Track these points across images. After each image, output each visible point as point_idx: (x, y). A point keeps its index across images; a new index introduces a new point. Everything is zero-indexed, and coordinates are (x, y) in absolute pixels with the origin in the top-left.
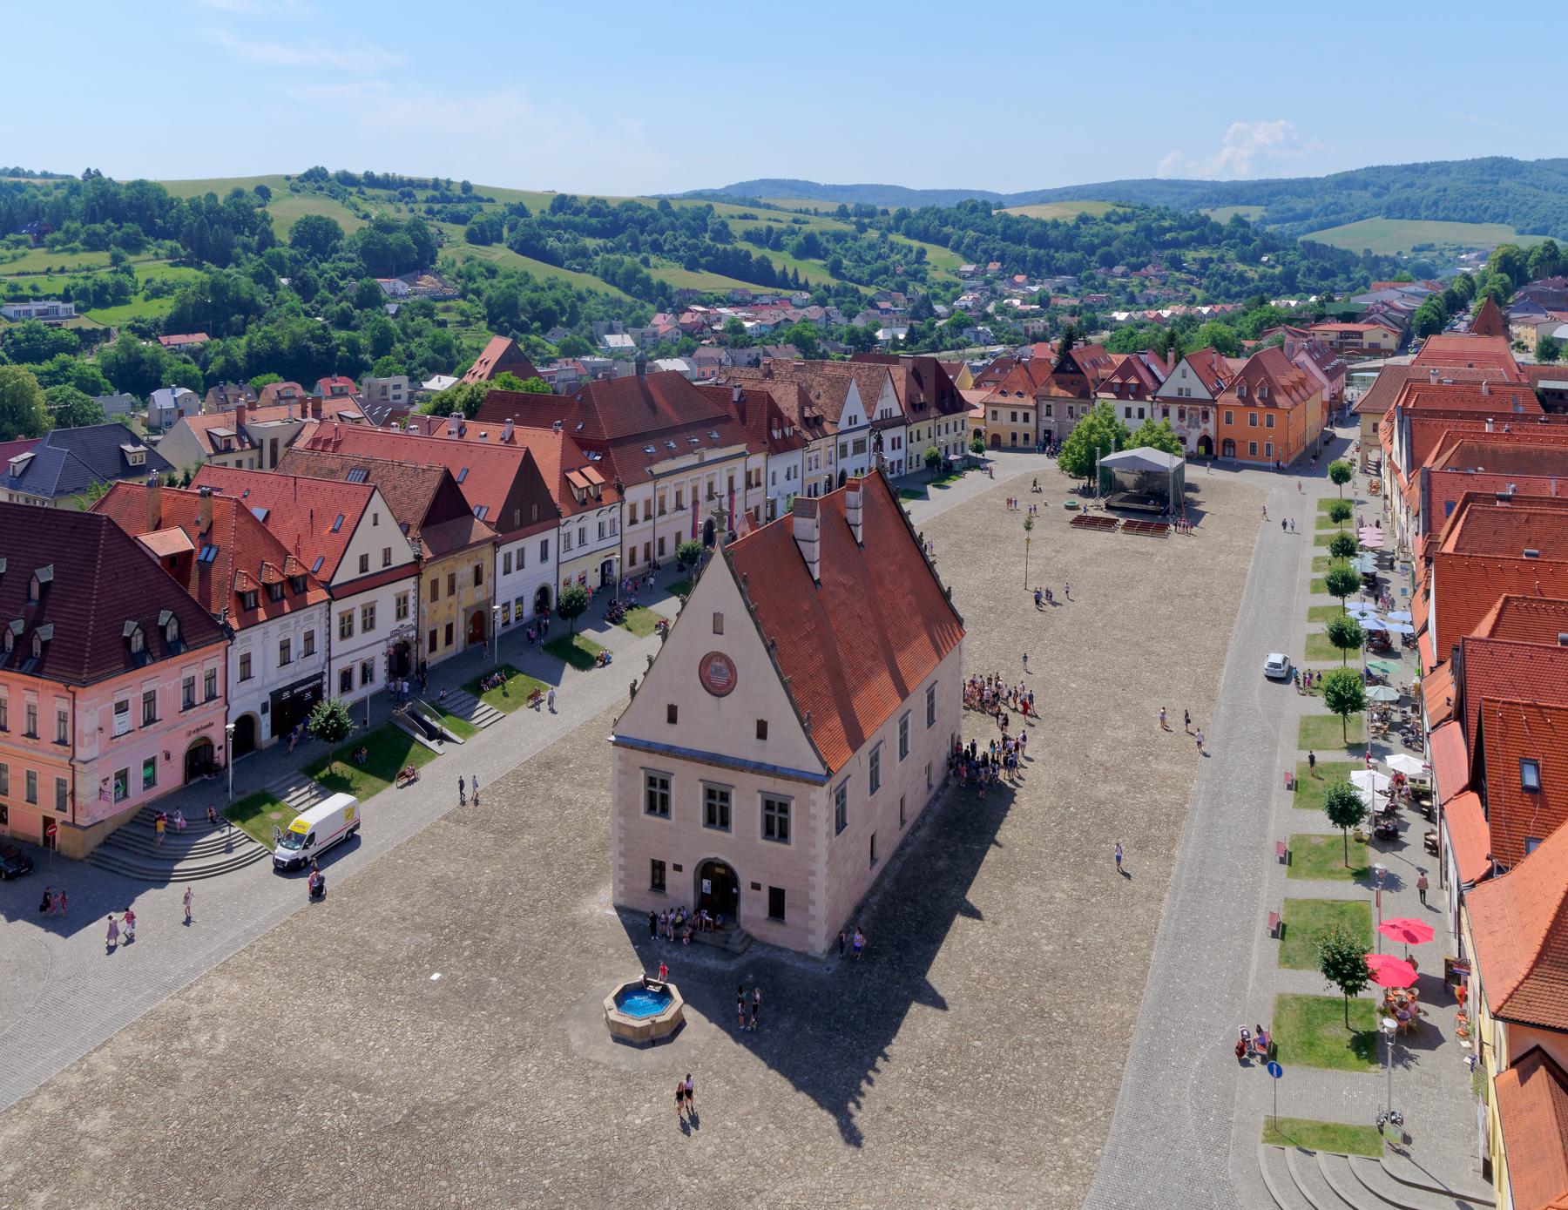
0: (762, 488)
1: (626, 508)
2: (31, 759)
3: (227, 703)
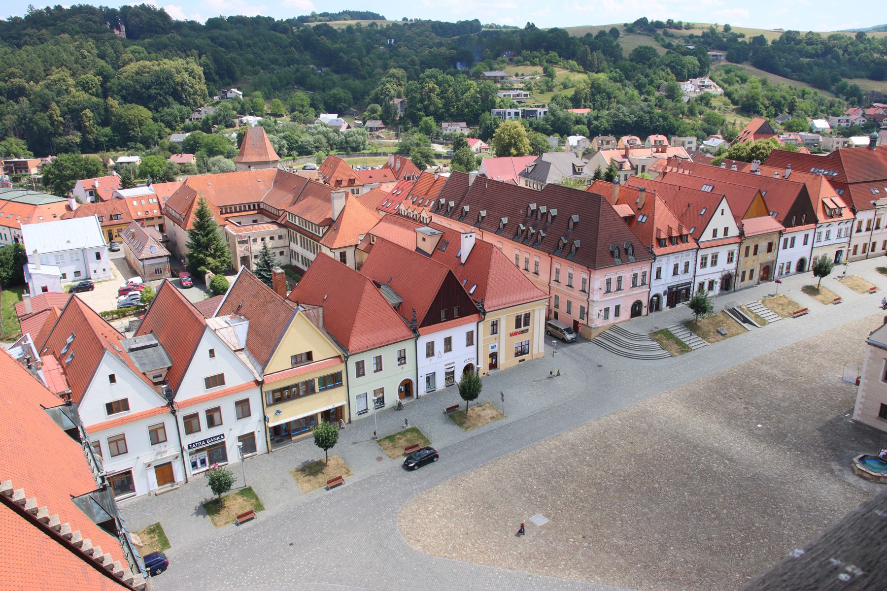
1: (856, 223)
2: (569, 295)
3: (650, 288)
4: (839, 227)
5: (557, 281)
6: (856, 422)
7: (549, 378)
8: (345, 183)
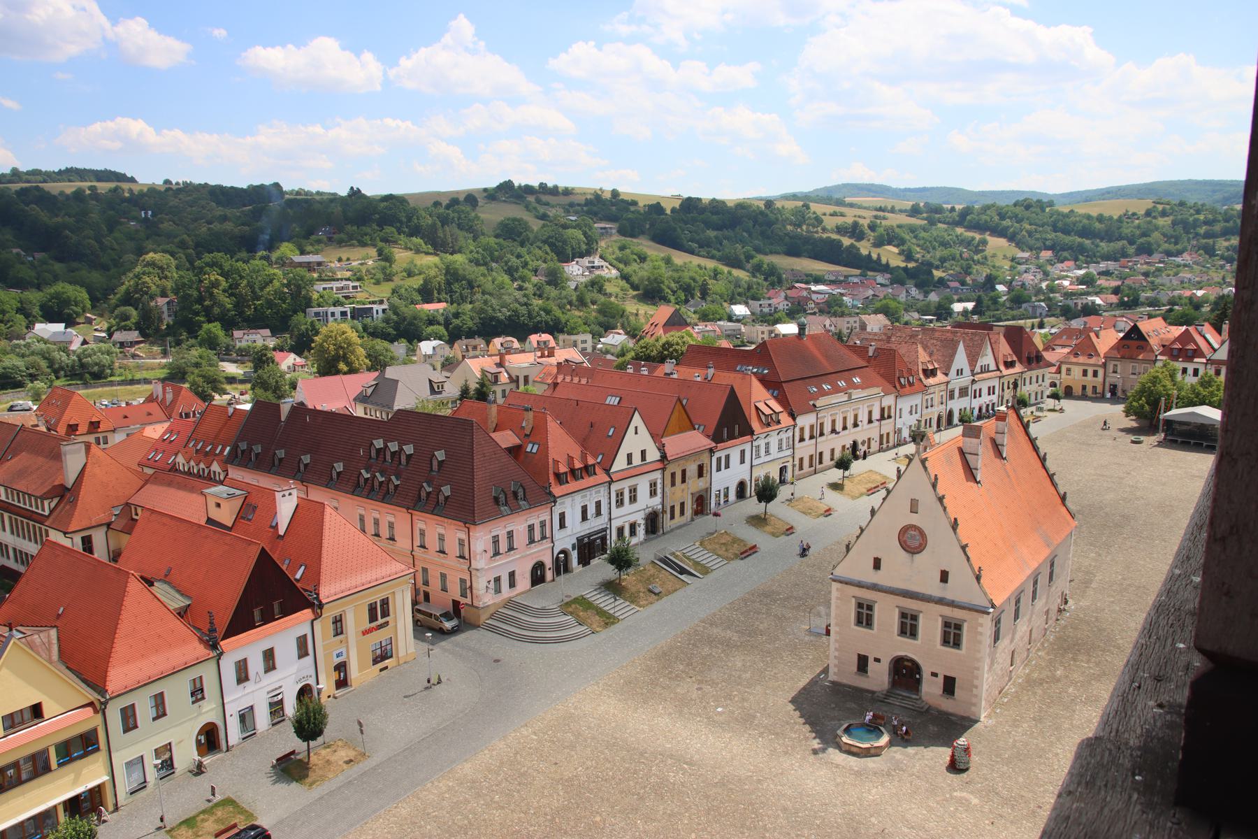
0: (891, 420)
1: (797, 430)
2: (443, 565)
3: (552, 542)
4: (779, 437)
5: (423, 546)
6: (833, 682)
7: (427, 688)
8: (83, 428)
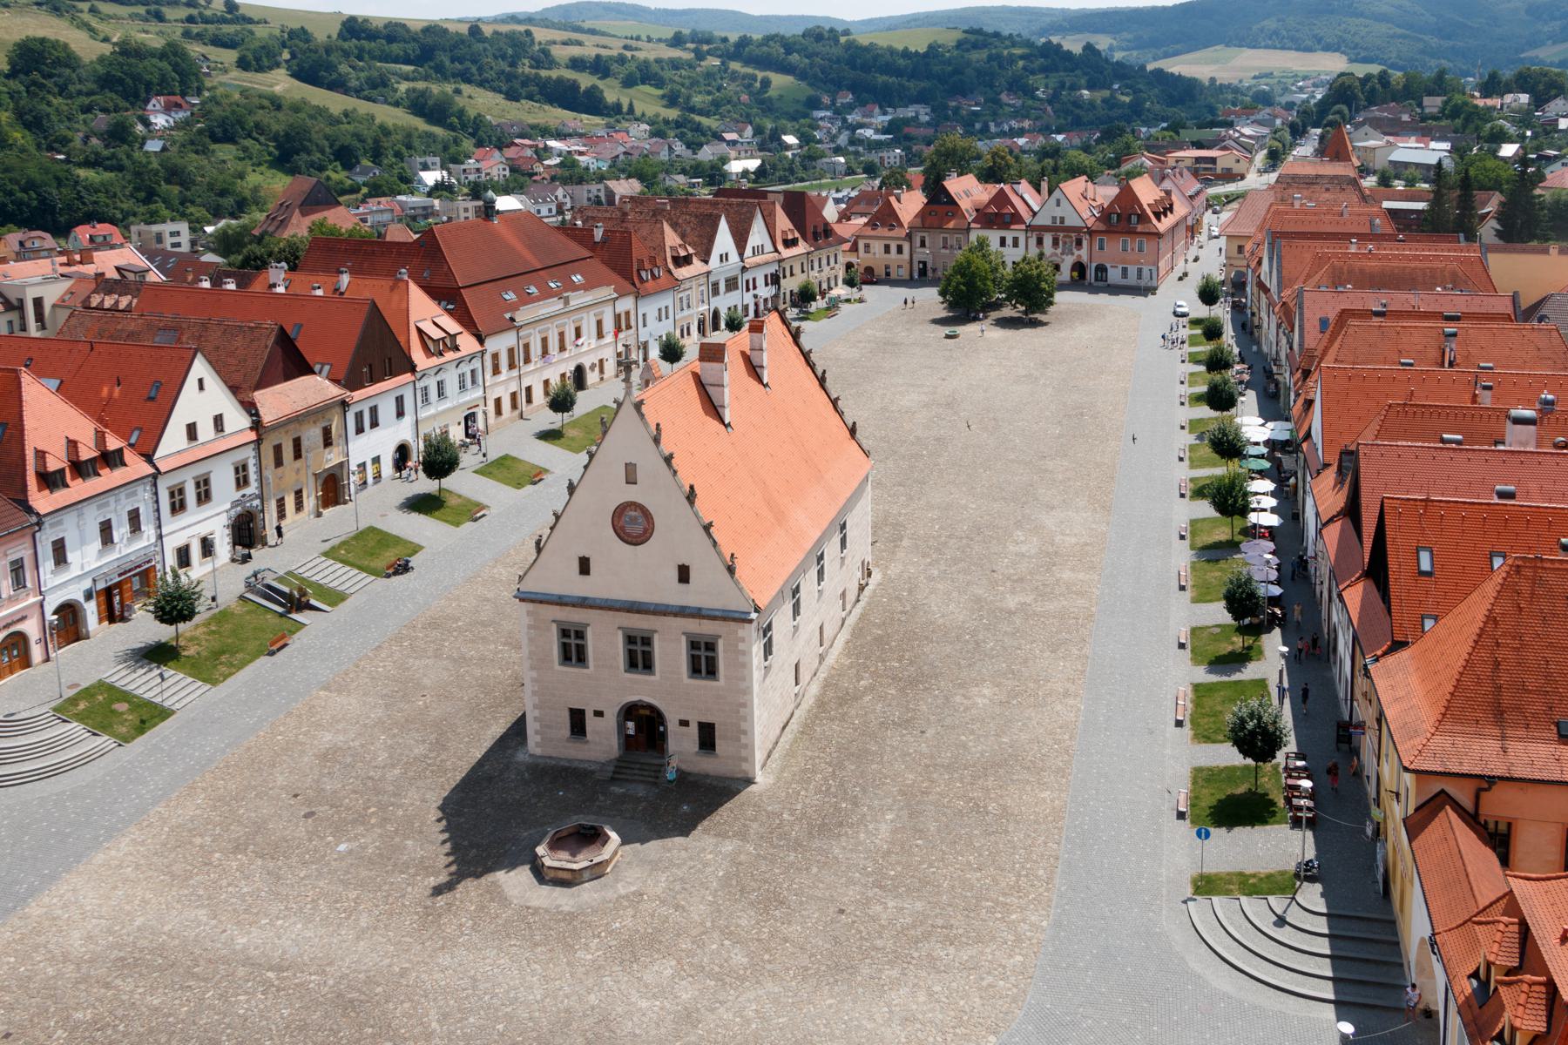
0: (632, 331)
1: (488, 358)
4: (460, 371)
